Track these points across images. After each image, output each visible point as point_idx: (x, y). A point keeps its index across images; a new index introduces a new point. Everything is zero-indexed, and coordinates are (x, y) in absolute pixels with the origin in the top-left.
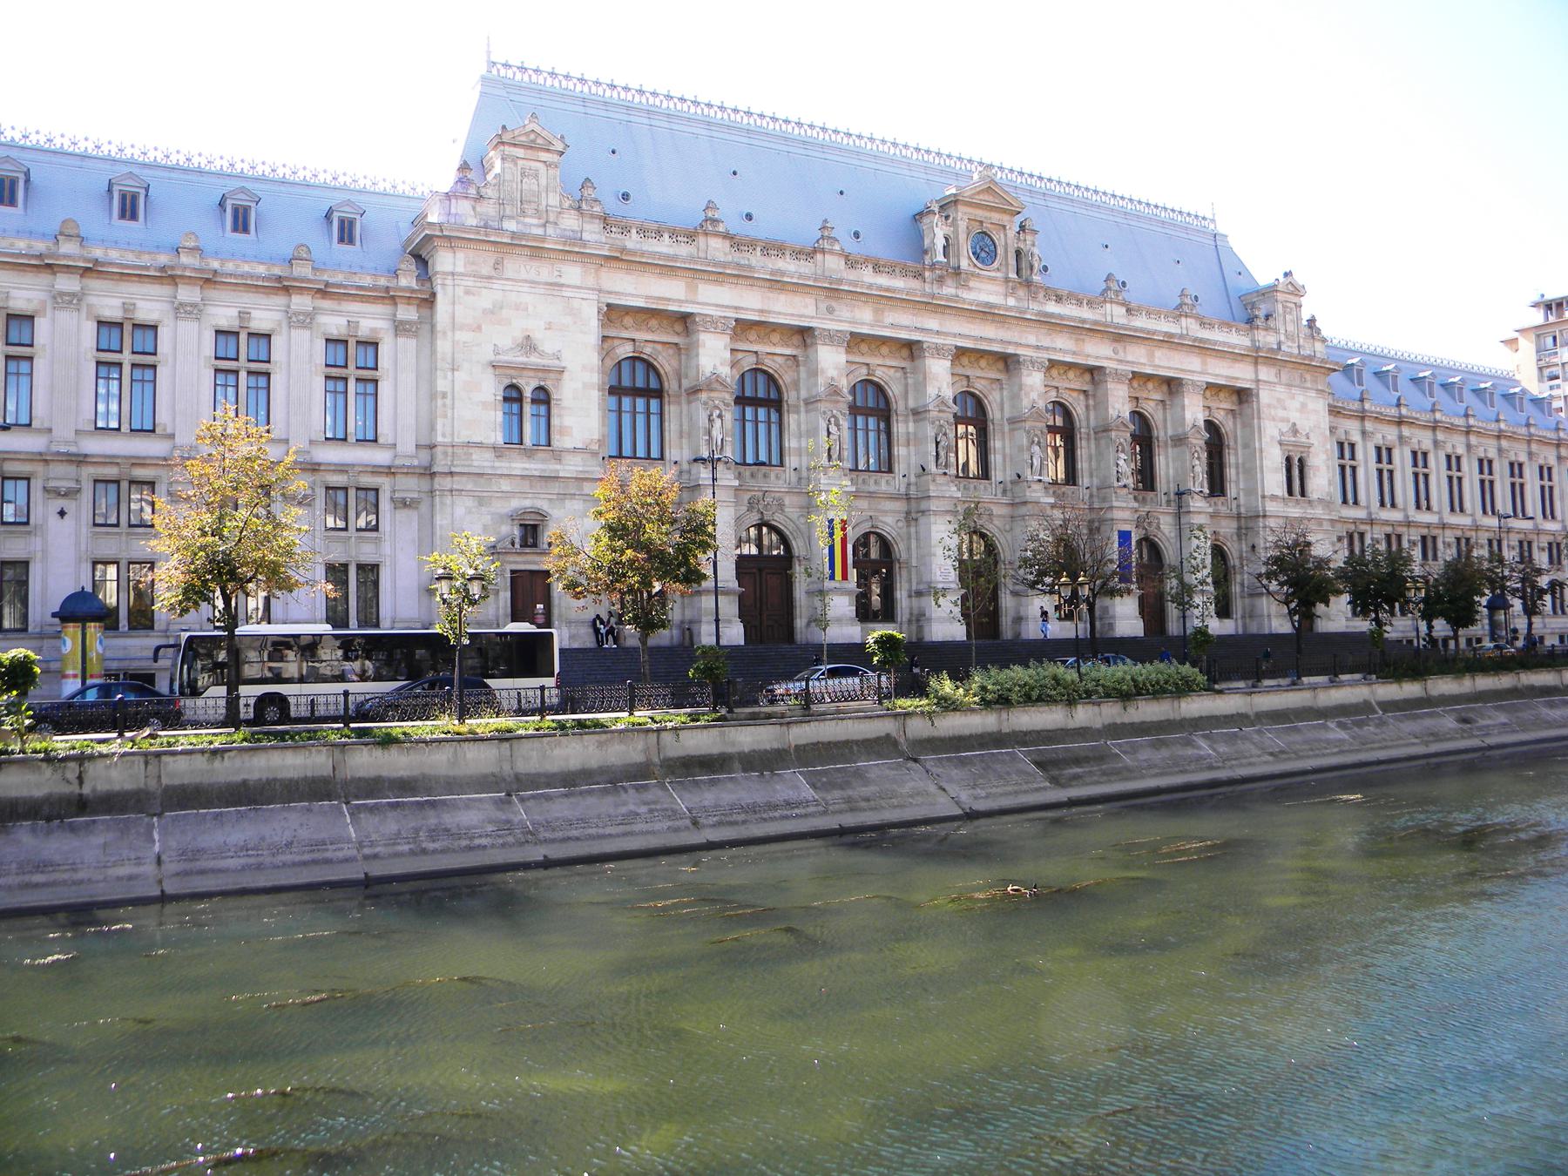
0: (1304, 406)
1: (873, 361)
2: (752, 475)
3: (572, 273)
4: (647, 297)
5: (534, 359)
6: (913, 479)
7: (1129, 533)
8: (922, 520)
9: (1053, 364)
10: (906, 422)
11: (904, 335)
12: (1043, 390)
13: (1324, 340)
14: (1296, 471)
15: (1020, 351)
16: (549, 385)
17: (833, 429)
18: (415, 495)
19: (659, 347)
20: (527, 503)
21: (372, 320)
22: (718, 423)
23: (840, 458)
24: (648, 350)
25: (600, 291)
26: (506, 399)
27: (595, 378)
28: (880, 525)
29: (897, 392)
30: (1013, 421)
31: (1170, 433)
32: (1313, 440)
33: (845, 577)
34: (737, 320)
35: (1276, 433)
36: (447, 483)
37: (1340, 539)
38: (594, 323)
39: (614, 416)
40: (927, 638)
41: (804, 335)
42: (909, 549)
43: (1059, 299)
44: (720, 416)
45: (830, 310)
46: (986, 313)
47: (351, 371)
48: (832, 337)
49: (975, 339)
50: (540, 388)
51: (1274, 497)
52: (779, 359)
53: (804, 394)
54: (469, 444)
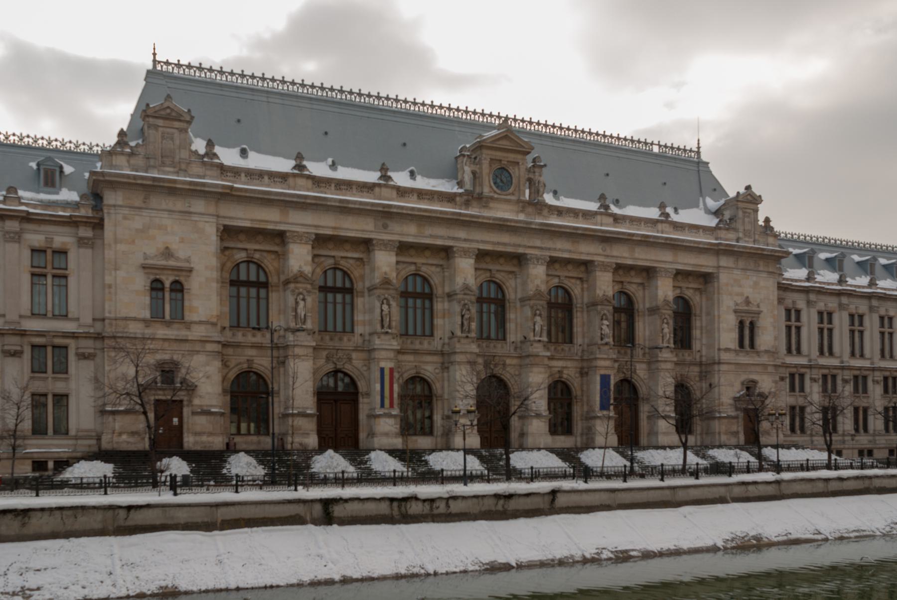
0: (756, 284)
1: (420, 260)
2: (331, 339)
3: (199, 205)
4: (252, 220)
5: (172, 263)
6: (446, 341)
8: (452, 368)
10: (443, 302)
11: (439, 242)
12: (544, 277)
13: (776, 236)
14: (747, 332)
15: (528, 251)
16: (182, 279)
17: (385, 307)
18: (92, 351)
19: (265, 254)
20: (167, 357)
21: (62, 238)
22: (302, 304)
23: (390, 327)
24: (257, 256)
25: (218, 216)
26: (152, 289)
27: (215, 274)
28: (422, 371)
29: (437, 282)
30: (522, 300)
31: (647, 305)
32: (763, 308)
34: (316, 235)
37: (782, 379)
38: (214, 238)
39: (235, 300)
41: (366, 244)
42: (443, 387)
44: (304, 300)
45: (385, 226)
46: (501, 226)
48: (386, 245)
49: (494, 243)
50: (176, 282)
51: (727, 350)
52: (351, 261)
53: (367, 284)
54: (126, 319)
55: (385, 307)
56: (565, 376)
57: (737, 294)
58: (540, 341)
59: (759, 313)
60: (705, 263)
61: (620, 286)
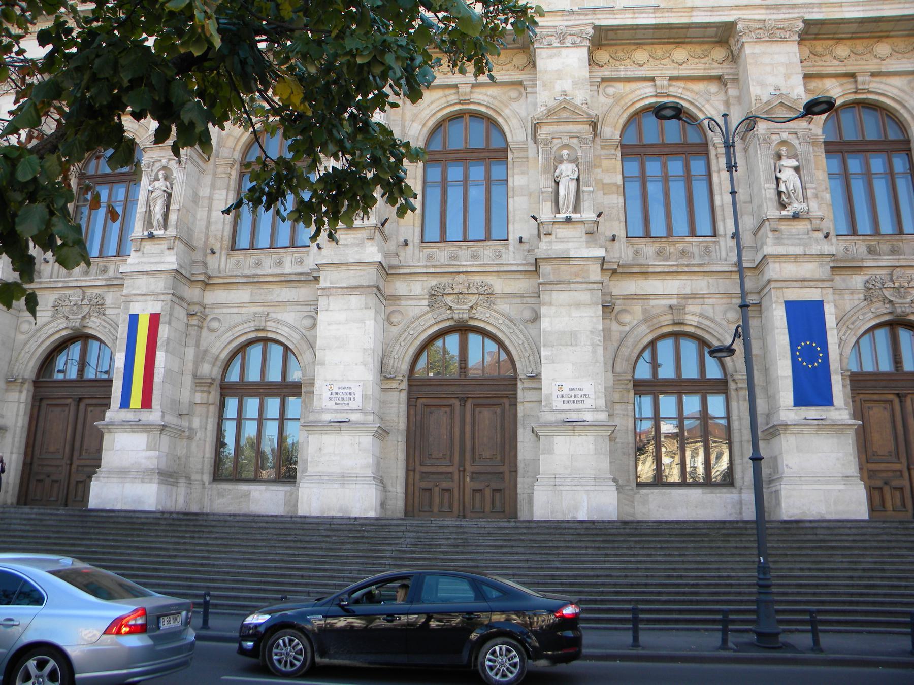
7: (818, 306)
23: (165, 225)
28: (271, 326)
33: (147, 403)
40: (301, 512)
55: (161, 184)
56: (692, 319)
58: (568, 220)
61: (850, 87)
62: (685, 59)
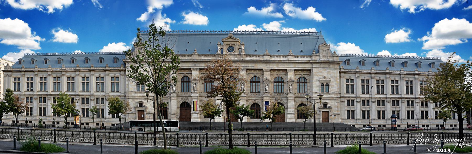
0: (329, 72)
7: (268, 102)
9: (247, 69)
32: (332, 80)
35: (318, 79)
36: (127, 97)
43: (250, 56)
47: (115, 81)
57: (320, 75)
59: (330, 81)
60: (307, 67)
62: (258, 72)
